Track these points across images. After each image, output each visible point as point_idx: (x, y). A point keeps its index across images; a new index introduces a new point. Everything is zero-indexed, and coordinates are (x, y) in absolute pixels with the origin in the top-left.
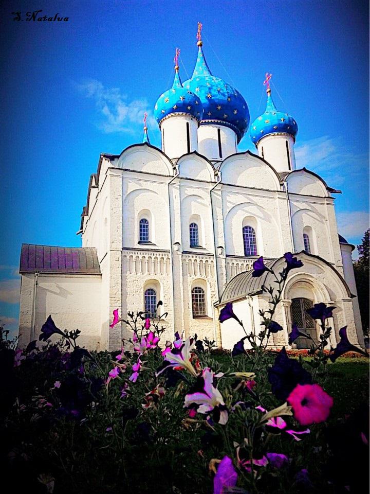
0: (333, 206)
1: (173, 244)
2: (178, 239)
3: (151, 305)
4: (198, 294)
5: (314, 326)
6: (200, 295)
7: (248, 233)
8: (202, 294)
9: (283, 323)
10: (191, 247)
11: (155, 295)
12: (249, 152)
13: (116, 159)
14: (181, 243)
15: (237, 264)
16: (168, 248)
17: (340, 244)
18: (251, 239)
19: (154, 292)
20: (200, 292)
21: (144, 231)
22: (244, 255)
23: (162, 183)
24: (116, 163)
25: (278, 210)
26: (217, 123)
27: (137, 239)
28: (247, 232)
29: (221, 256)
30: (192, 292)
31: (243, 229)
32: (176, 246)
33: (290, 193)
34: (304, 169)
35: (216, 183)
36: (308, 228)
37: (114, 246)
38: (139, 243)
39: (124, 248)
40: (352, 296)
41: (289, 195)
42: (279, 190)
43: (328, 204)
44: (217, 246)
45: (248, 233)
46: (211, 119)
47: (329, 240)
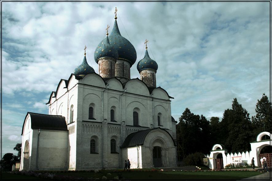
3: (93, 146)
7: (136, 115)
10: (111, 121)
15: (130, 129)
20: (114, 141)
22: (132, 124)
24: (82, 82)
26: (123, 60)
27: (88, 116)
31: (134, 112)
33: (154, 98)
34: (160, 87)
36: (160, 114)
38: (89, 119)
39: (83, 121)
45: (136, 115)
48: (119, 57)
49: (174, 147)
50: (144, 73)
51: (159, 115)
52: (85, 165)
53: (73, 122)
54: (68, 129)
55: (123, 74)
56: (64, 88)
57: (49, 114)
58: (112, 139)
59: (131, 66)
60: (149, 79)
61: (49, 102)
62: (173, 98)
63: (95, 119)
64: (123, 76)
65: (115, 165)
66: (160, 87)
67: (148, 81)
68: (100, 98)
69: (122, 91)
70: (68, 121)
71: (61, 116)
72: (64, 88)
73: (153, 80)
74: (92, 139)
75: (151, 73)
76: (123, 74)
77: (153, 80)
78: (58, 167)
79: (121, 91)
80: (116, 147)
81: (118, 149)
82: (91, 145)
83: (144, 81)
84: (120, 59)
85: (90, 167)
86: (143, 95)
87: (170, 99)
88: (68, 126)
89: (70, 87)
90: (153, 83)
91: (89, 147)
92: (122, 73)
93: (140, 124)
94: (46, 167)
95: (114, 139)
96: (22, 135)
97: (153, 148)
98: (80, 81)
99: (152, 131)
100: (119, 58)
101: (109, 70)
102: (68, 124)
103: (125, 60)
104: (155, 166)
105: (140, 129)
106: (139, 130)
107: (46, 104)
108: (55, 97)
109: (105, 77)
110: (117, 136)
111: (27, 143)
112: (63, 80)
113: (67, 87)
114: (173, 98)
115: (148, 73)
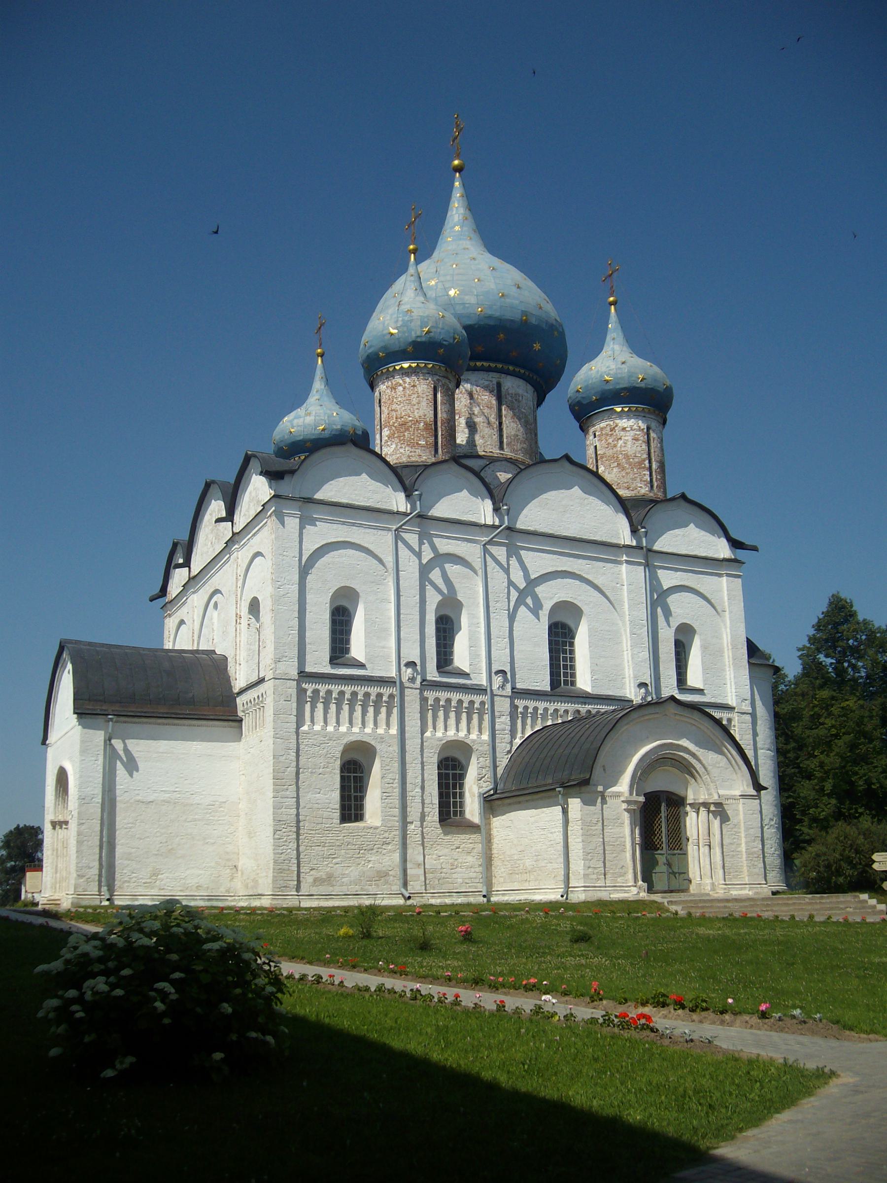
0: (740, 580)
1: (403, 663)
2: (412, 653)
3: (353, 794)
4: (451, 772)
5: (683, 846)
6: (454, 775)
8: (458, 772)
9: (625, 842)
11: (362, 773)
12: (567, 458)
13: (287, 478)
14: (418, 663)
16: (393, 673)
17: (748, 661)
18: (565, 652)
19: (360, 766)
20: (454, 768)
21: (341, 632)
23: (384, 529)
24: (287, 487)
25: (625, 587)
26: (495, 370)
28: (557, 634)
29: (500, 692)
30: (439, 768)
32: (410, 670)
35: (498, 527)
37: (282, 668)
40: (759, 787)
41: (650, 554)
42: (628, 542)
43: (728, 575)
44: (494, 671)
46: (486, 360)
47: (728, 655)
48: (471, 359)
49: (754, 793)
50: (602, 429)
51: (680, 638)
52: (315, 880)
53: (261, 681)
54: (240, 714)
55: (501, 442)
56: (219, 520)
57: (168, 645)
58: (447, 759)
59: (540, 400)
60: (627, 457)
61: (164, 591)
62: (754, 549)
63: (362, 666)
64: (501, 448)
65: (460, 880)
66: (683, 497)
67: (624, 469)
68: (380, 561)
69: (489, 522)
70: (240, 677)
71: (213, 652)
72: (219, 520)
73: (650, 462)
74: (349, 757)
75: (640, 429)
76: (501, 442)
77: (650, 462)
78: (198, 887)
79: (485, 526)
80: (467, 795)
81: (472, 809)
82: (343, 788)
83: (601, 469)
84: (482, 369)
85: (337, 890)
86: (597, 538)
87: (741, 554)
88: (239, 700)
89: (241, 518)
90: (651, 475)
91: (336, 795)
92: (496, 437)
93: (584, 682)
94: (141, 891)
95: (454, 760)
96: (44, 742)
97: (642, 799)
98: (281, 482)
99: (634, 715)
100: (479, 364)
101: (426, 423)
102: (242, 692)
103: (508, 373)
104: (650, 890)
105: (584, 709)
106: (578, 711)
107: (152, 600)
108: (187, 564)
109: (404, 460)
110: (466, 741)
111: (62, 777)
112: (213, 482)
113: (230, 516)
114: (754, 549)
115: (624, 429)
